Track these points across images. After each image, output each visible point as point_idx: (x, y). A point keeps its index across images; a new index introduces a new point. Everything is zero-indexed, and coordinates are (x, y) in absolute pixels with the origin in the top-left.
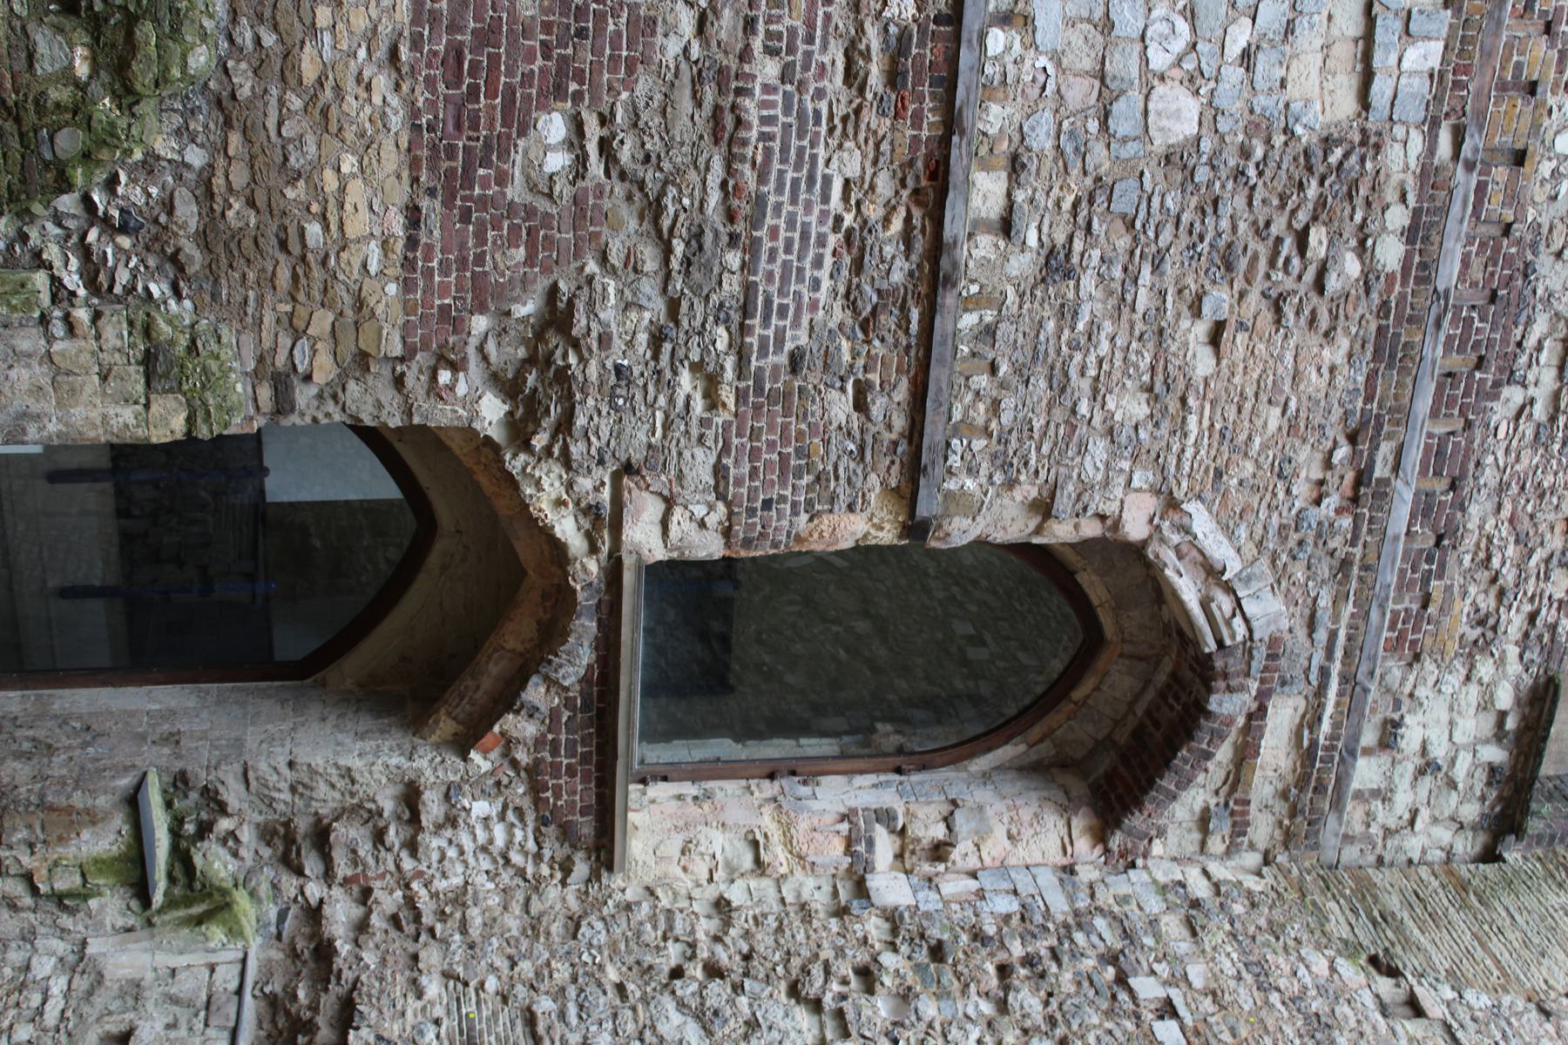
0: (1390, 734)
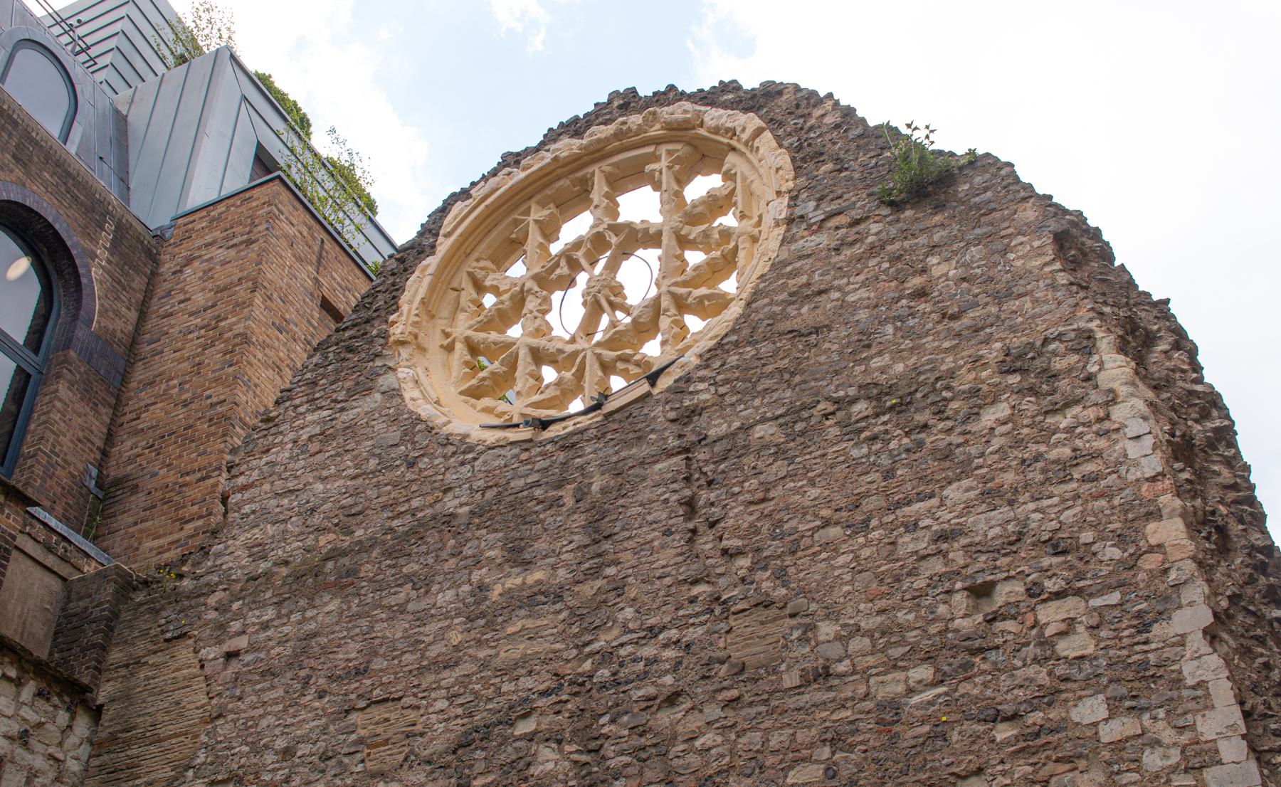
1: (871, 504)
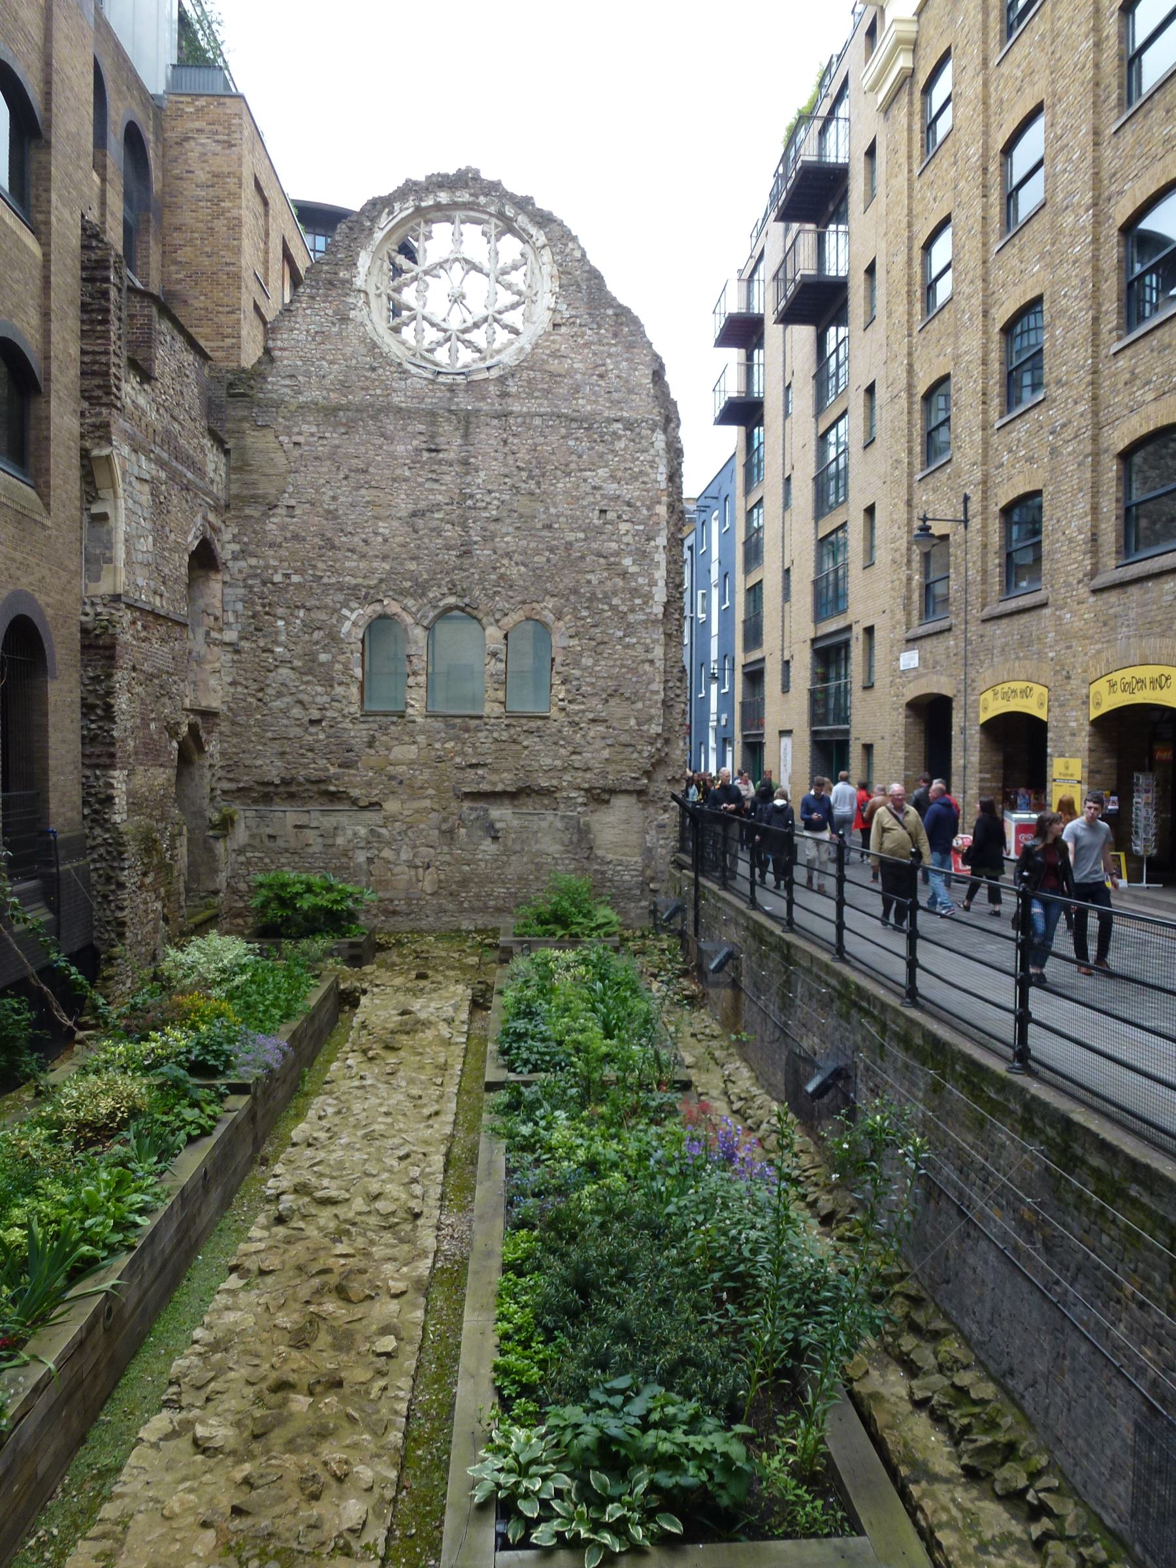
0: (212, 481)
1: (573, 466)
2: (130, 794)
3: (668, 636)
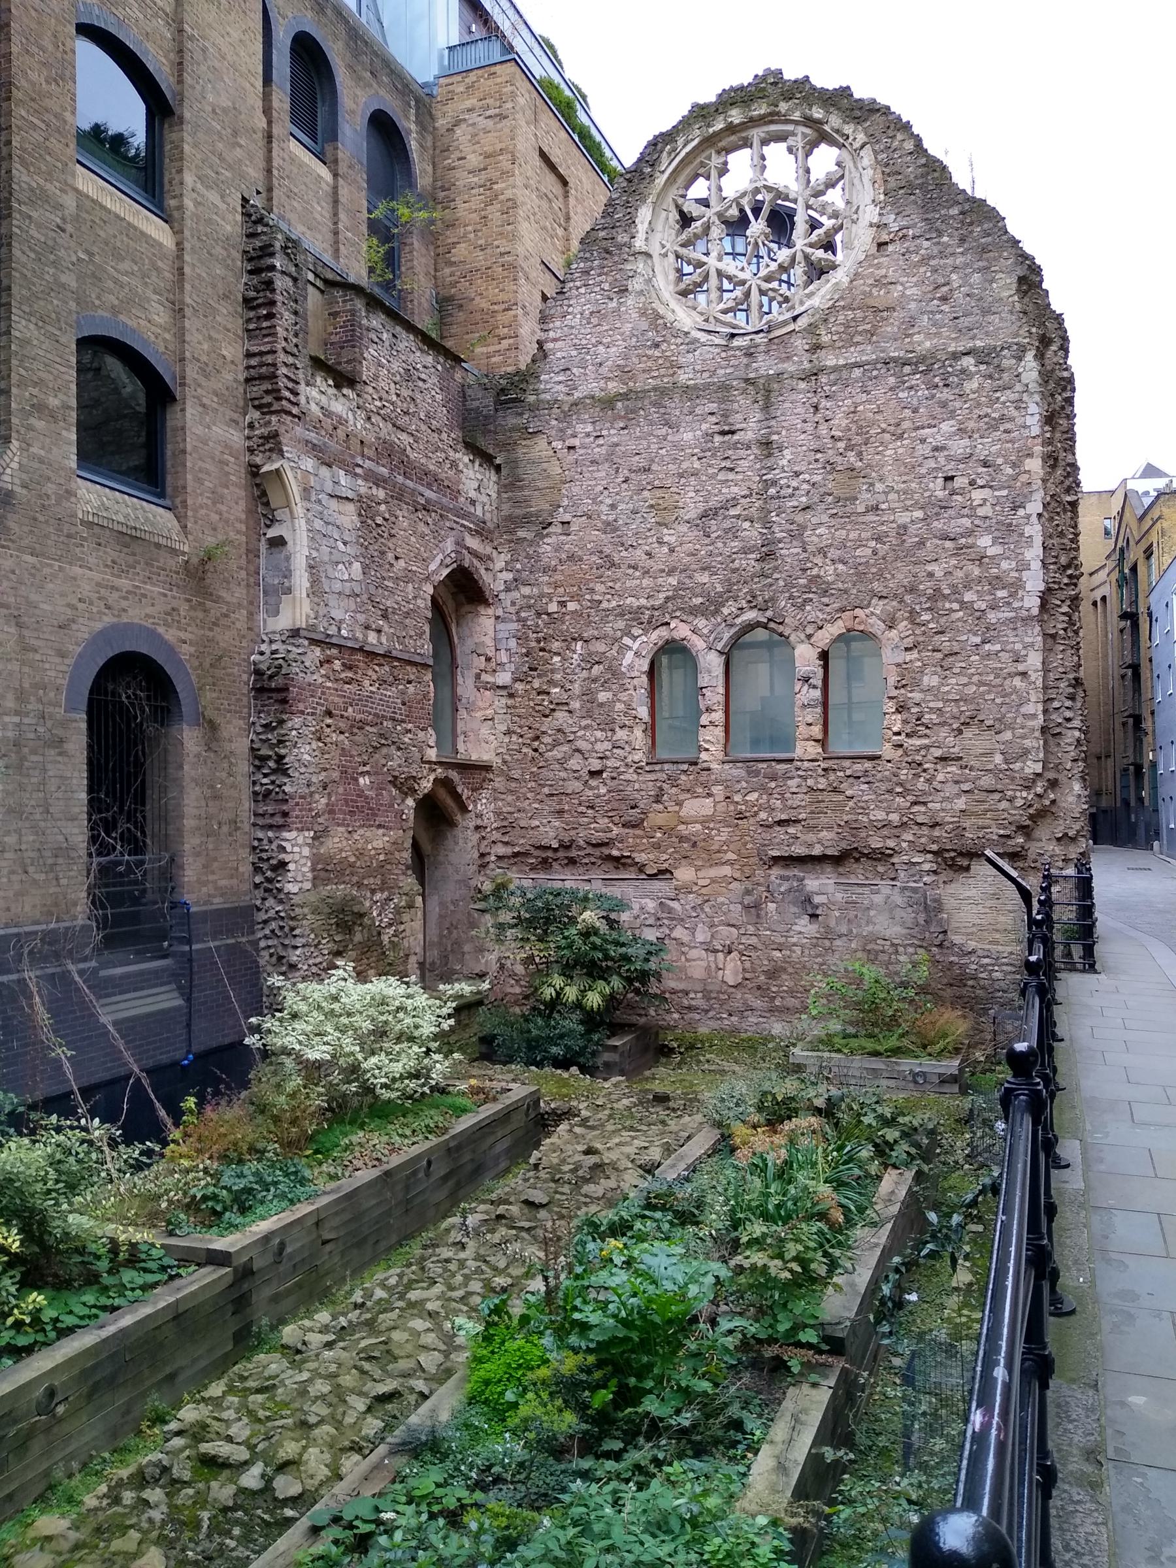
0: (473, 502)
1: (906, 425)
2: (316, 859)
3: (1051, 637)
